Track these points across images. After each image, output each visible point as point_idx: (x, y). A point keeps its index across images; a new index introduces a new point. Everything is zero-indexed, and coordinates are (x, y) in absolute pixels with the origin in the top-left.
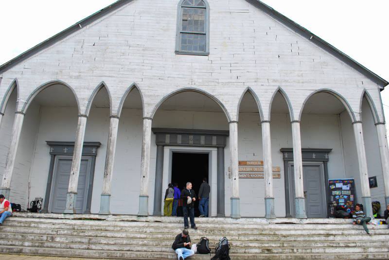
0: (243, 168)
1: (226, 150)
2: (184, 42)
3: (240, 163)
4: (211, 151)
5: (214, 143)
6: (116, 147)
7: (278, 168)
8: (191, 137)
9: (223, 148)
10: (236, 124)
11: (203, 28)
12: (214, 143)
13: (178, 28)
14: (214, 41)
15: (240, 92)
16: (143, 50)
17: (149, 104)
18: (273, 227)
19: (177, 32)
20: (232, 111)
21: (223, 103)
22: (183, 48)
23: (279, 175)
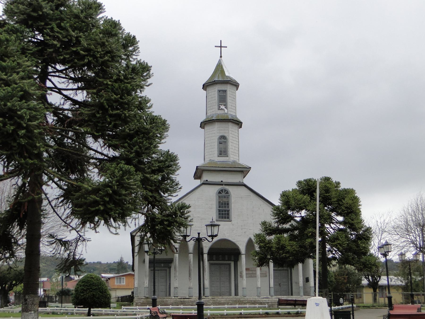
0: (248, 272)
1: (238, 263)
2: (219, 214)
3: (247, 269)
4: (231, 263)
5: (233, 259)
6: (179, 261)
7: (266, 271)
8: (220, 256)
9: (237, 262)
10: (244, 255)
11: (229, 207)
12: (233, 259)
13: (217, 208)
14: (234, 213)
15: (246, 240)
16: (201, 219)
17: (206, 247)
18: (260, 299)
19: (216, 210)
20: (243, 249)
21: (238, 245)
22: (219, 217)
23: (266, 275)
